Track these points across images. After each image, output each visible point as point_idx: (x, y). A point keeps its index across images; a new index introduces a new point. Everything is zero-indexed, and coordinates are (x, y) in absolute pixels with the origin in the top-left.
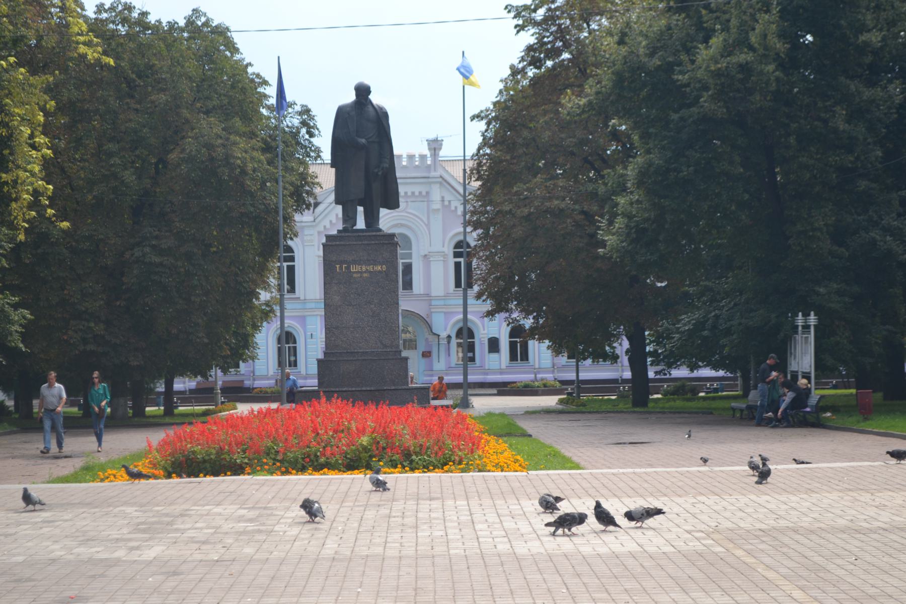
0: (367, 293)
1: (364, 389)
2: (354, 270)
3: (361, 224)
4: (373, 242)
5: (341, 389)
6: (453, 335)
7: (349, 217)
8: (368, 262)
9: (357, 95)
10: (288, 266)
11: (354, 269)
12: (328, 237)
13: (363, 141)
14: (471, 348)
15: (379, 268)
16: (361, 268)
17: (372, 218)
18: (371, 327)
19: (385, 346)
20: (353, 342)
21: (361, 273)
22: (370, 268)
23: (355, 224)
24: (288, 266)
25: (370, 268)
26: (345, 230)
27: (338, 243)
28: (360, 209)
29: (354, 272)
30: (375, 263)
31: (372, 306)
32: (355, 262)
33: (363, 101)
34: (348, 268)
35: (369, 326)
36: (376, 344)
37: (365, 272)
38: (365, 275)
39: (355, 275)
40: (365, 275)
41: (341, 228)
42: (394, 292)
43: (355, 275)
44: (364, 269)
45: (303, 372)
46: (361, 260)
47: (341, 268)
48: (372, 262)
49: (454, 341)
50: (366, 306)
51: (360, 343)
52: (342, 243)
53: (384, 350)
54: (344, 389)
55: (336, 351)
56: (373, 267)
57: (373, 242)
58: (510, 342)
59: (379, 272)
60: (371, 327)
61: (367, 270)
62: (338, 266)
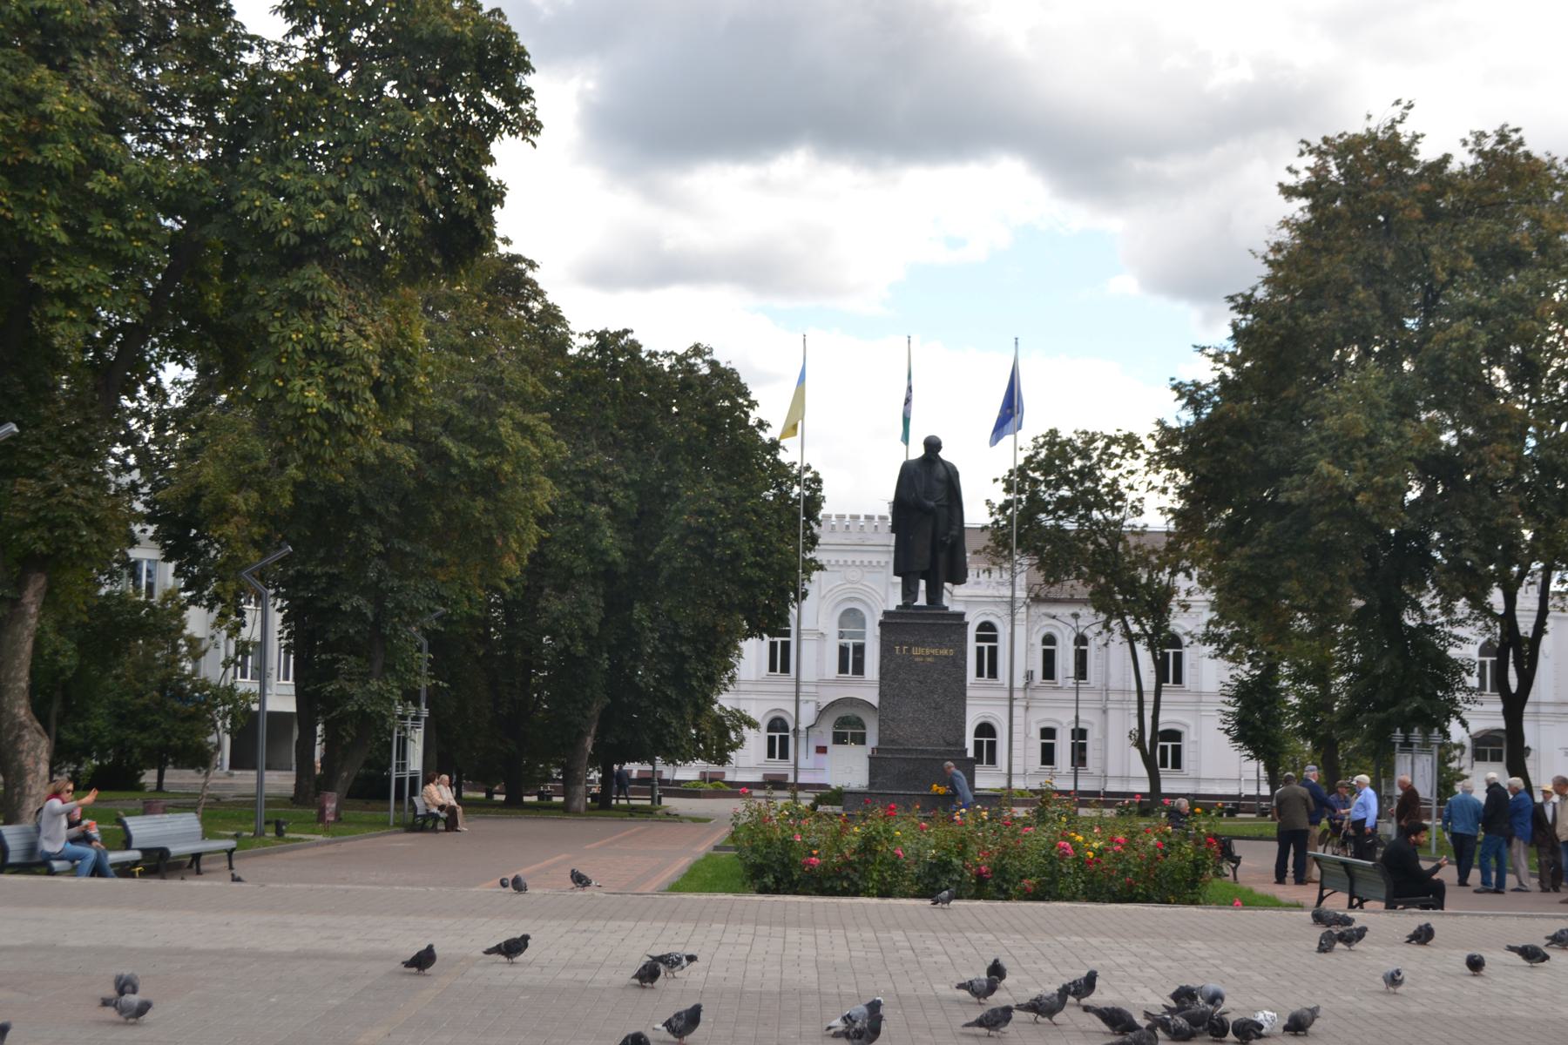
3: (922, 600)
7: (909, 592)
9: (926, 450)
10: (782, 642)
11: (916, 651)
12: (886, 613)
13: (932, 504)
17: (934, 594)
19: (949, 744)
21: (924, 657)
22: (934, 651)
23: (916, 600)
24: (782, 642)
25: (934, 651)
26: (906, 606)
28: (923, 584)
32: (917, 645)
34: (909, 650)
38: (929, 659)
40: (929, 659)
41: (900, 603)
43: (917, 659)
44: (928, 652)
47: (901, 650)
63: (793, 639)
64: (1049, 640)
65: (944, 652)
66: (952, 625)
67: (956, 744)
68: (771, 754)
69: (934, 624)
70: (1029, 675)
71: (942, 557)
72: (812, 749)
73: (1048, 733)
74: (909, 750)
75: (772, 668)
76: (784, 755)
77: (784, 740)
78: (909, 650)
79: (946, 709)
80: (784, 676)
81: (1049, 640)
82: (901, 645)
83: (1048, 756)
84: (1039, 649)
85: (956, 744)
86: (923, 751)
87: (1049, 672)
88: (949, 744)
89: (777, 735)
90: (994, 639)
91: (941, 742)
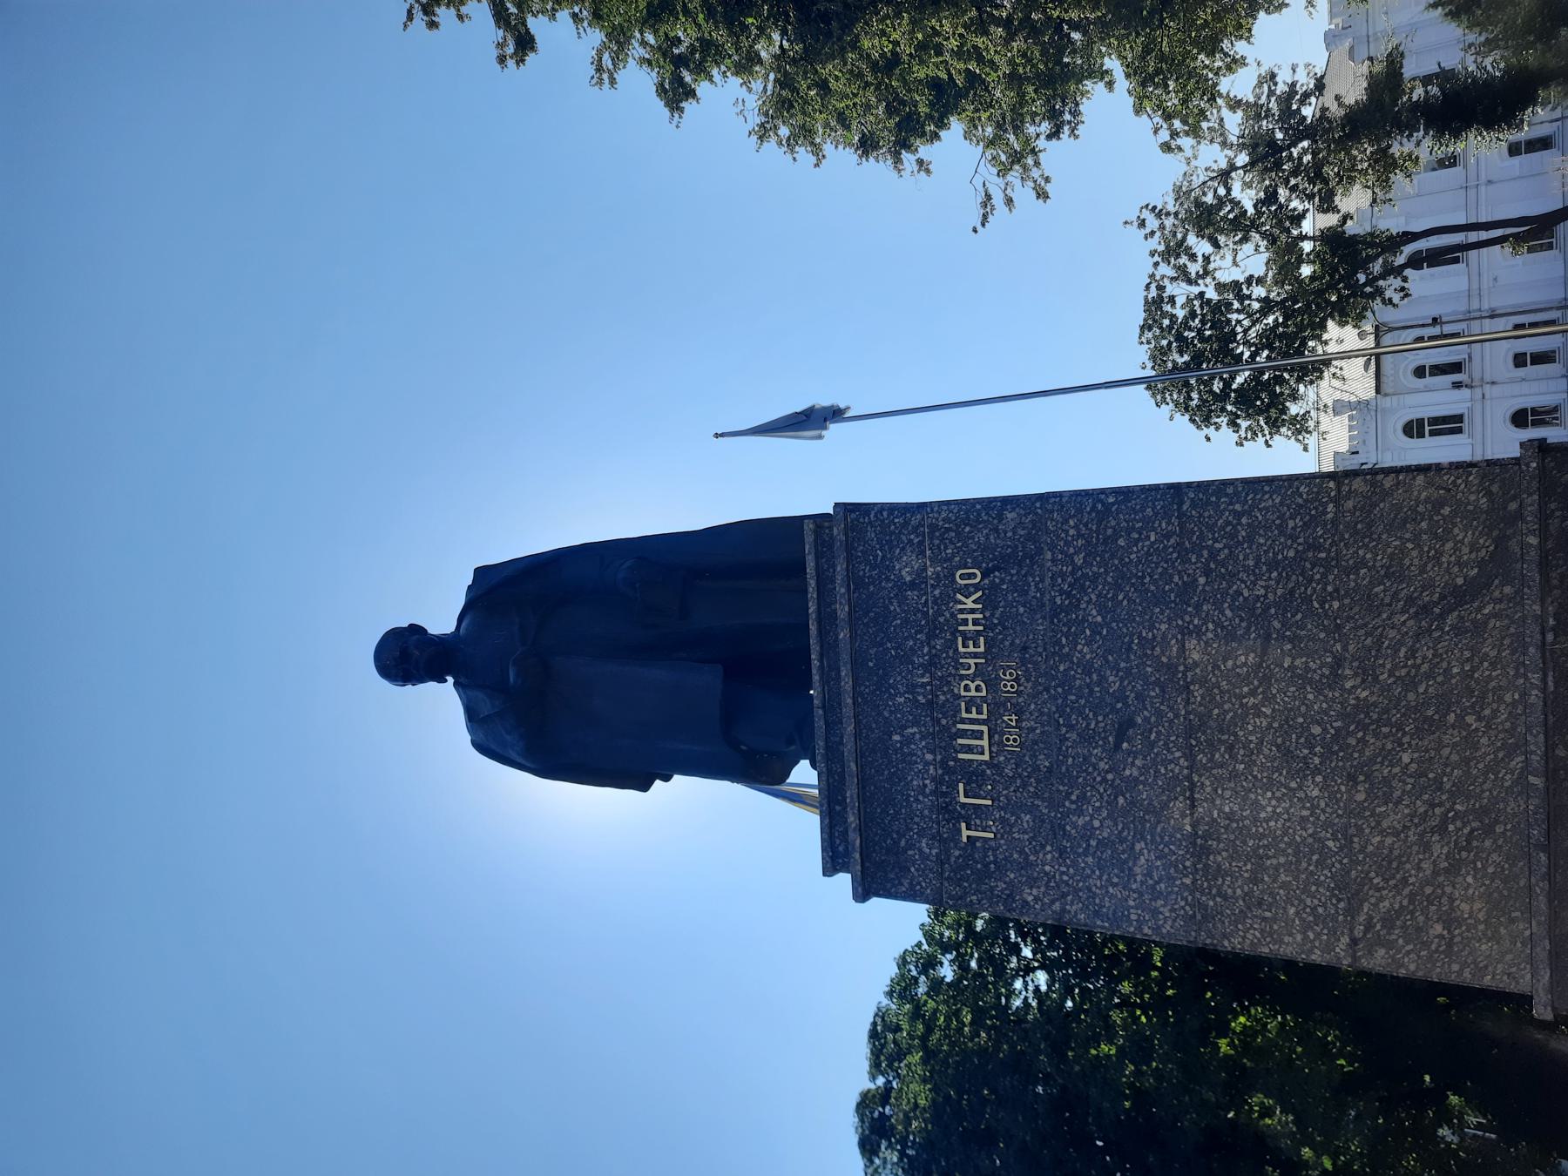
2: (985, 743)
8: (943, 667)
11: (978, 751)
15: (969, 603)
16: (970, 703)
18: (1338, 662)
19: (1498, 564)
21: (997, 708)
22: (971, 653)
25: (971, 653)
27: (852, 819)
29: (997, 745)
30: (943, 628)
32: (945, 739)
34: (974, 777)
35: (1335, 678)
36: (1479, 628)
37: (992, 684)
39: (1012, 740)
40: (1008, 685)
43: (1012, 740)
44: (974, 689)
46: (930, 703)
47: (973, 816)
48: (939, 643)
50: (1198, 692)
51: (1470, 742)
56: (963, 633)
58: (1531, 364)
59: (988, 602)
60: (1338, 662)
61: (979, 673)
62: (965, 833)
64: (1420, 372)
70: (1457, 385)
73: (1520, 360)
81: (1420, 372)
82: (951, 813)
83: (1541, 358)
84: (1429, 380)
87: (1456, 367)
90: (1420, 422)
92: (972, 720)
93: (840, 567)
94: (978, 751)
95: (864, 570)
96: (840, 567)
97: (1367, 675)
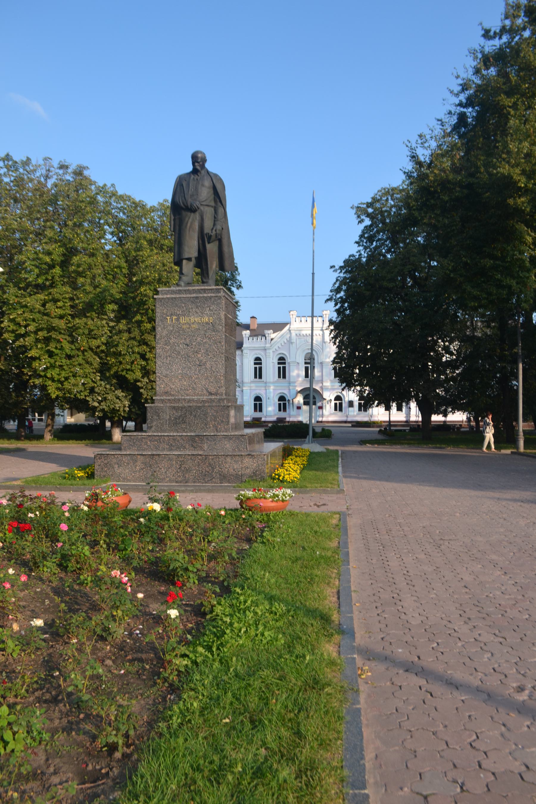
0: (194, 344)
1: (189, 434)
4: (201, 295)
5: (163, 434)
6: (333, 399)
11: (182, 320)
14: (341, 404)
19: (211, 394)
20: (181, 389)
27: (168, 296)
31: (199, 356)
33: (198, 168)
34: (178, 320)
37: (193, 323)
42: (220, 343)
43: (184, 327)
45: (265, 414)
49: (333, 402)
52: (173, 296)
53: (210, 397)
54: (166, 434)
55: (165, 397)
57: (201, 295)
59: (207, 323)
62: (168, 318)
63: (287, 366)
65: (206, 319)
66: (210, 298)
67: (216, 394)
68: (280, 410)
69: (197, 298)
71: (212, 248)
72: (295, 408)
74: (179, 400)
75: (279, 377)
76: (285, 410)
77: (285, 405)
78: (178, 320)
79: (208, 365)
80: (284, 380)
85: (216, 394)
86: (189, 401)
88: (211, 394)
89: (282, 403)
91: (205, 392)
92: (187, 319)
93: (213, 295)
94: (182, 320)
95: (213, 300)
96: (213, 295)
97: (197, 378)
